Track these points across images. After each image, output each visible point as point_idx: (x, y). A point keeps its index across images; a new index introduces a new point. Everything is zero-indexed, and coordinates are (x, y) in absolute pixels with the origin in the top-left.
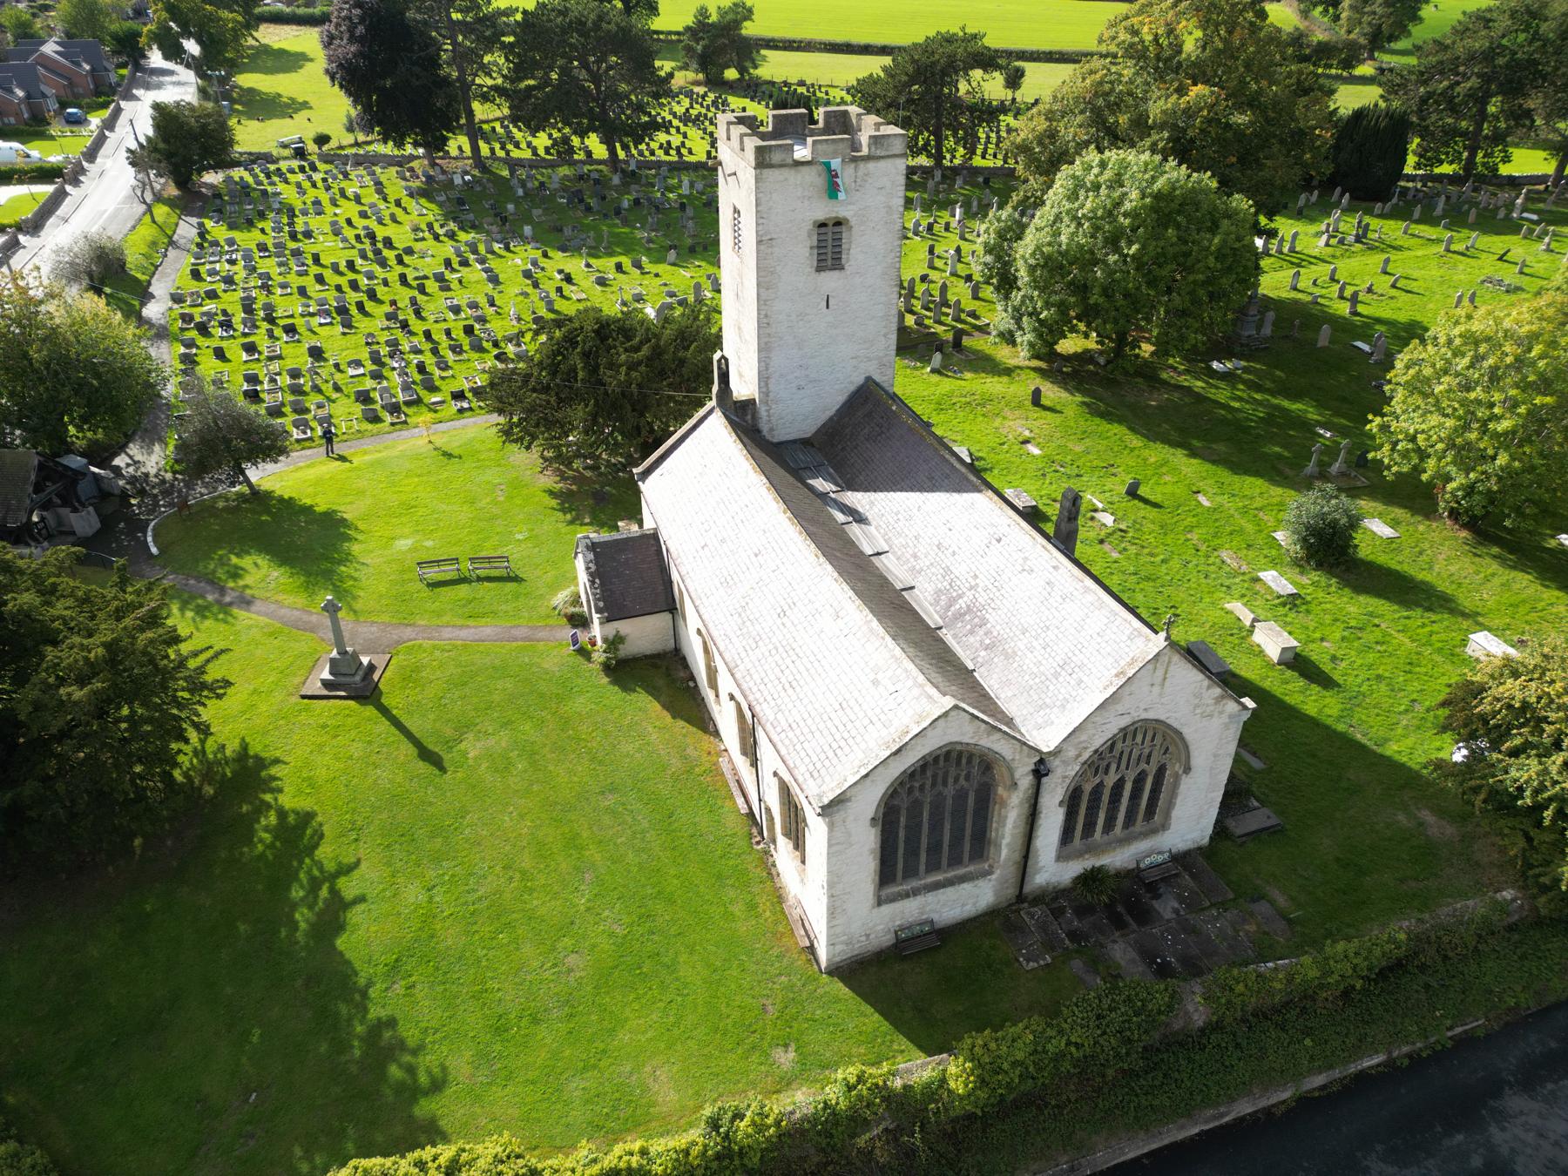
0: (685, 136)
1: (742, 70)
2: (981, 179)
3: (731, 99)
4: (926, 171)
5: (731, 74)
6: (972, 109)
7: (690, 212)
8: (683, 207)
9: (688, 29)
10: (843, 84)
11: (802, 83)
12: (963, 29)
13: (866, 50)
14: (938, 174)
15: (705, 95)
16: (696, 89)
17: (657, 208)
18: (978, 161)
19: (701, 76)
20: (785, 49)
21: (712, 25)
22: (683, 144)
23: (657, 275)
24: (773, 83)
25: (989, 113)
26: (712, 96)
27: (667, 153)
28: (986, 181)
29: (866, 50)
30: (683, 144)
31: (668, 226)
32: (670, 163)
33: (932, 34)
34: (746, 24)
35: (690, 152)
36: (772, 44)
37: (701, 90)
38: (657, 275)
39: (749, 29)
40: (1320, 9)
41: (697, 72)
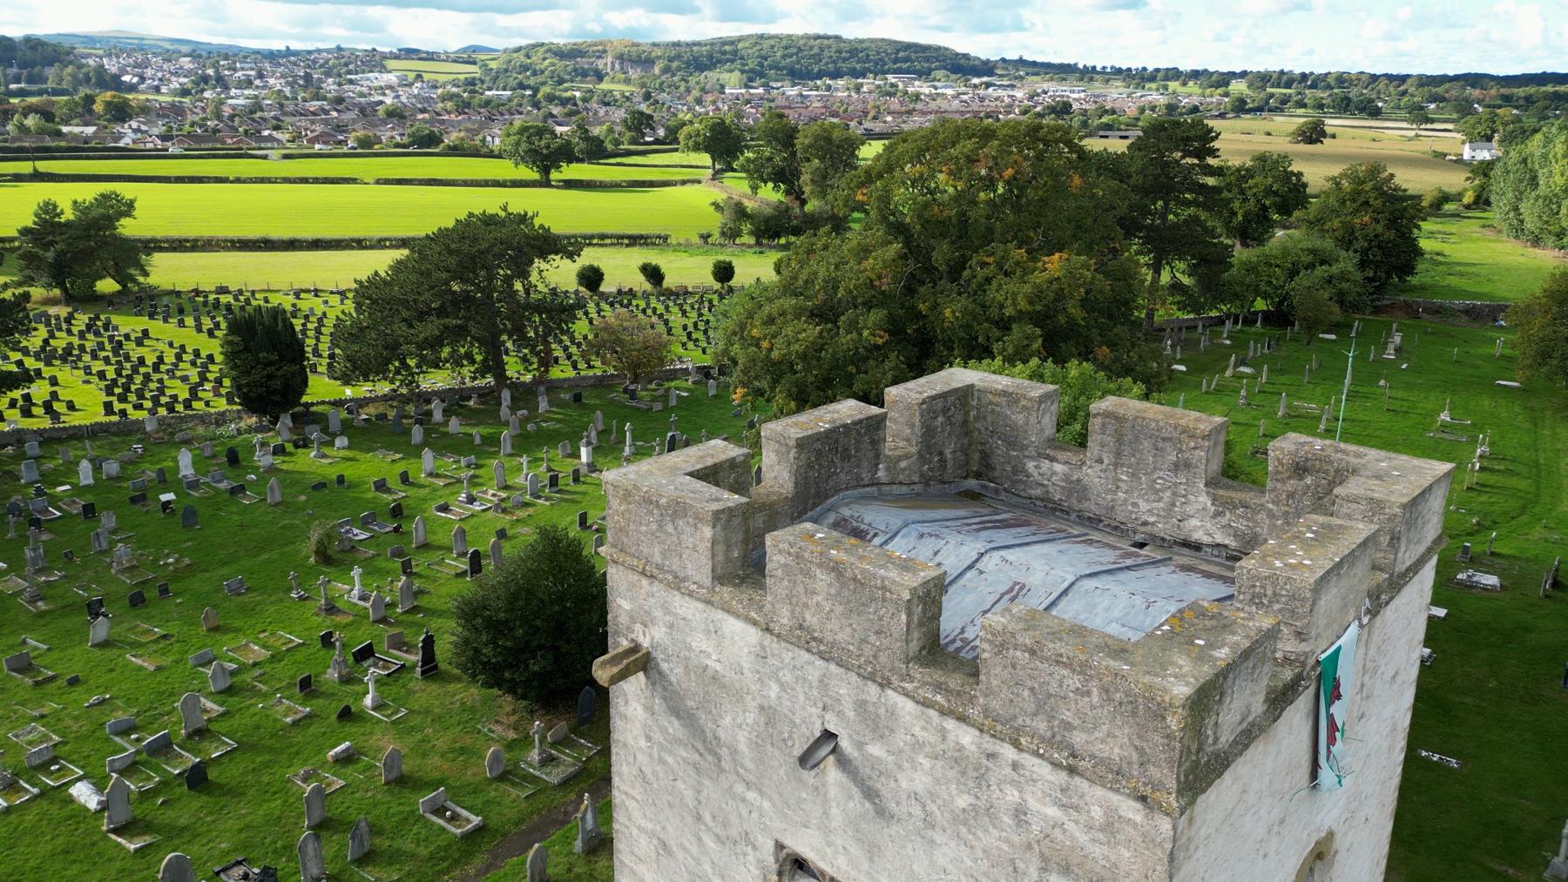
0: (54, 381)
1: (123, 279)
2: (566, 396)
3: (116, 319)
4: (487, 395)
5: (107, 285)
6: (539, 307)
7: (108, 520)
8: (89, 511)
9: (25, 232)
10: (286, 287)
11: (223, 290)
12: (505, 209)
13: (359, 244)
14: (506, 395)
15: (69, 320)
16: (52, 311)
17: (36, 523)
18: (556, 373)
19: (57, 292)
20: (174, 250)
21: (68, 224)
22: (54, 396)
23: (74, 681)
24: (178, 294)
25: (559, 310)
26: (81, 320)
27: (27, 413)
28: (577, 398)
29: (380, 244)
30: (54, 396)
31: (69, 557)
32: (40, 432)
33: (463, 216)
34: (124, 221)
35: (71, 406)
36: (153, 245)
37: (63, 311)
38: (74, 681)
39: (128, 228)
40: (770, 185)
41: (49, 286)
